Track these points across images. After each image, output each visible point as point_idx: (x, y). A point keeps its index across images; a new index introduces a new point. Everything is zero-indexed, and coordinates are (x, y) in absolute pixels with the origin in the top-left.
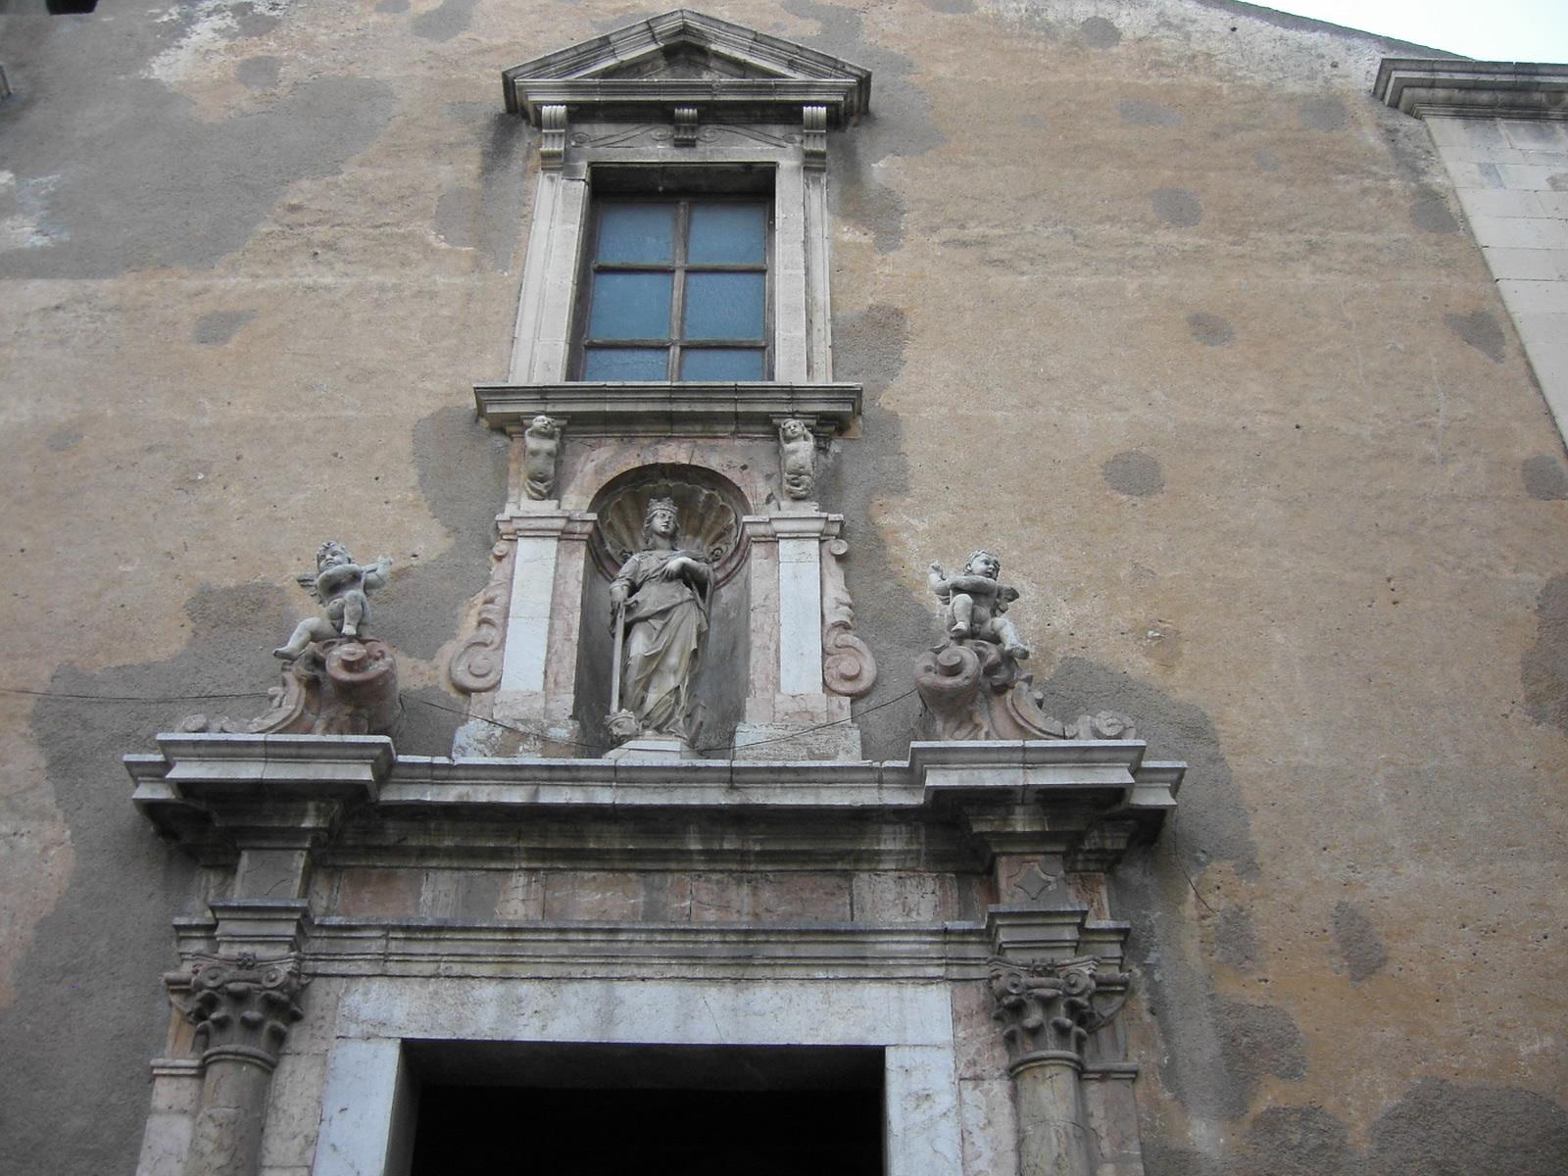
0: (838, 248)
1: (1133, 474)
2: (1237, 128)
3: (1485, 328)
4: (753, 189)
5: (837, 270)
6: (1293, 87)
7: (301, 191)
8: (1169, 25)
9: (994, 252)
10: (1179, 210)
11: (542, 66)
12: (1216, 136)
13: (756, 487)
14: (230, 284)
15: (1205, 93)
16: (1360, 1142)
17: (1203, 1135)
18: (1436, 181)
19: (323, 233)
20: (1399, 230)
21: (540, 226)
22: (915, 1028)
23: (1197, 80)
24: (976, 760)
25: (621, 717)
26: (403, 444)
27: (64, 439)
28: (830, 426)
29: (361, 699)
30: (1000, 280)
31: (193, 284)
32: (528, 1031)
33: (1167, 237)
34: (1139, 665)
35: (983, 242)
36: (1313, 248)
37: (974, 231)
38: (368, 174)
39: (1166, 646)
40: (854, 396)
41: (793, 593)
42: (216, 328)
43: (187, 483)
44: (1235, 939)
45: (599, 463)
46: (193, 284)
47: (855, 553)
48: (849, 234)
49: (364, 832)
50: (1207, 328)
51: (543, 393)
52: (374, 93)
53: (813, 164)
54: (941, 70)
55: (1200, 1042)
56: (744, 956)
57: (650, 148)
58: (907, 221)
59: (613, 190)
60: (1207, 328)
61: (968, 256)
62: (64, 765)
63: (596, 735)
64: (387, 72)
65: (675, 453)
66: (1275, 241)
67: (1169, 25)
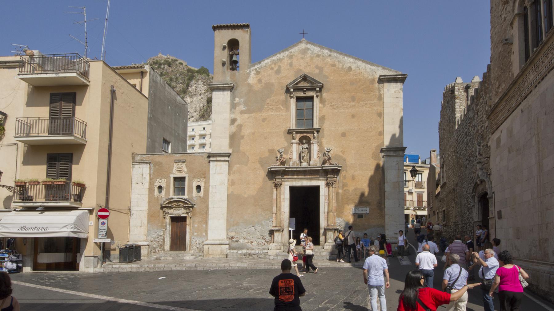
0: (320, 107)
1: (343, 135)
2: (362, 85)
3: (380, 115)
4: (311, 99)
5: (319, 110)
6: (370, 77)
7: (268, 101)
8: (358, 67)
9: (335, 107)
10: (353, 99)
11: (290, 84)
12: (359, 87)
13: (312, 138)
14: (264, 114)
15: (360, 79)
16: (351, 192)
17: (340, 191)
18: (382, 92)
19: (271, 107)
20: (376, 101)
21: (292, 106)
22: (321, 183)
23: (359, 77)
24: (327, 166)
25: (302, 161)
26: (282, 134)
27: (253, 134)
28: (318, 132)
29: (283, 163)
30: (335, 111)
31: (260, 115)
32: (297, 185)
33: (351, 104)
34: (341, 154)
35: (333, 106)
36: (366, 104)
37: (333, 104)
38: (274, 98)
39: (343, 152)
40: (320, 129)
41: (315, 148)
42: (264, 120)
43: (265, 139)
44: (345, 177)
45: (299, 136)
46: (260, 115)
47: (320, 145)
48: (321, 105)
49: (285, 173)
50: (353, 116)
51: (294, 130)
52: (272, 85)
53: (317, 96)
54: (332, 78)
55: (341, 185)
56: (311, 179)
57: (301, 94)
58: (326, 103)
59: (299, 99)
60: (353, 116)
61: (331, 108)
62: (262, 166)
63: (301, 163)
64: (273, 81)
65: (305, 134)
66: (362, 103)
67: (358, 67)
